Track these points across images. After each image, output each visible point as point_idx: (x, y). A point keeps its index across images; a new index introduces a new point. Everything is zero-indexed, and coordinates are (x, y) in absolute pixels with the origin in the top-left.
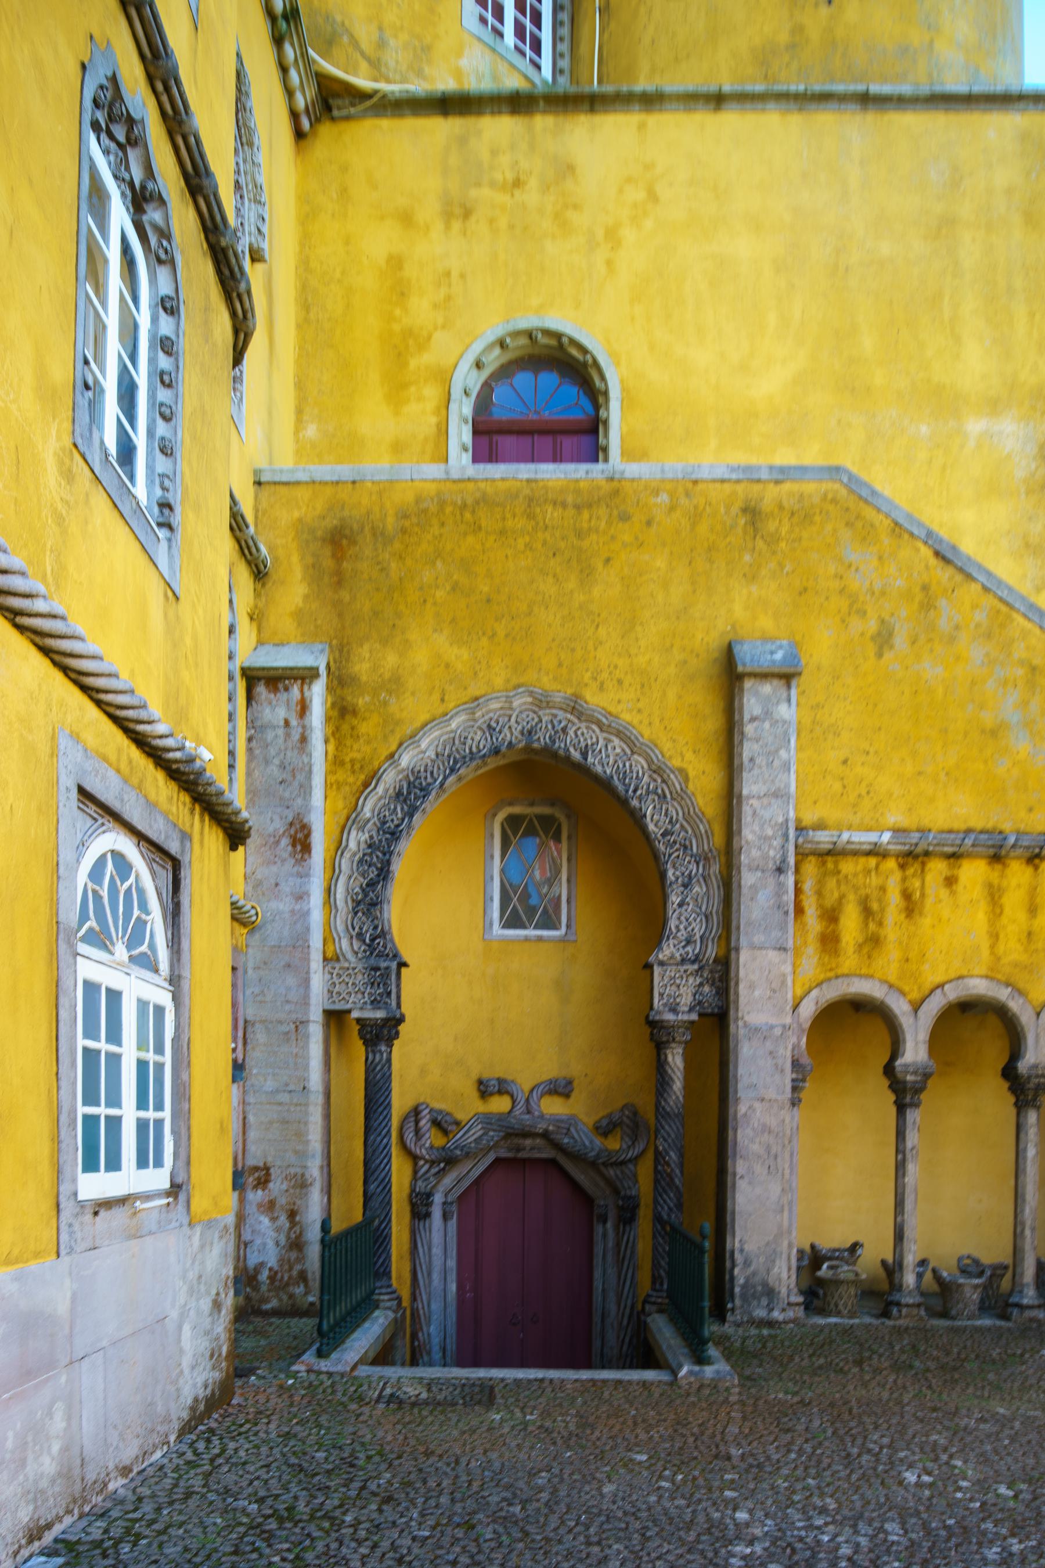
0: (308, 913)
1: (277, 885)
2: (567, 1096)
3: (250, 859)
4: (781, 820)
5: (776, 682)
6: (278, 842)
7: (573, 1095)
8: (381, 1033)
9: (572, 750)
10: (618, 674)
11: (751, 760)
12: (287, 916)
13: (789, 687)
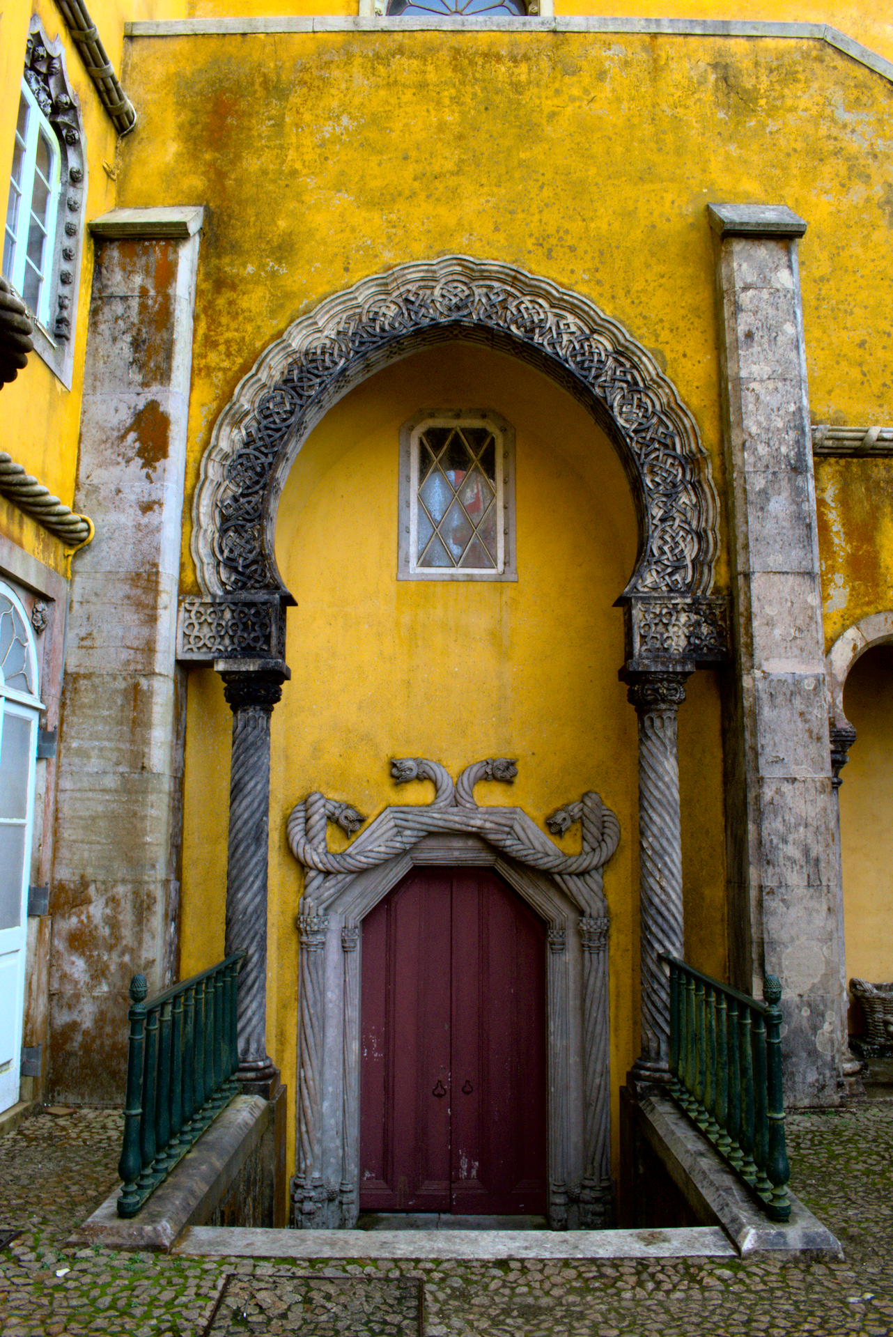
0: (158, 529)
1: (119, 491)
2: (509, 782)
3: (84, 460)
4: (792, 408)
5: (771, 245)
6: (123, 438)
7: (517, 780)
8: (258, 690)
9: (513, 328)
10: (570, 241)
11: (749, 335)
12: (130, 531)
13: (789, 252)
